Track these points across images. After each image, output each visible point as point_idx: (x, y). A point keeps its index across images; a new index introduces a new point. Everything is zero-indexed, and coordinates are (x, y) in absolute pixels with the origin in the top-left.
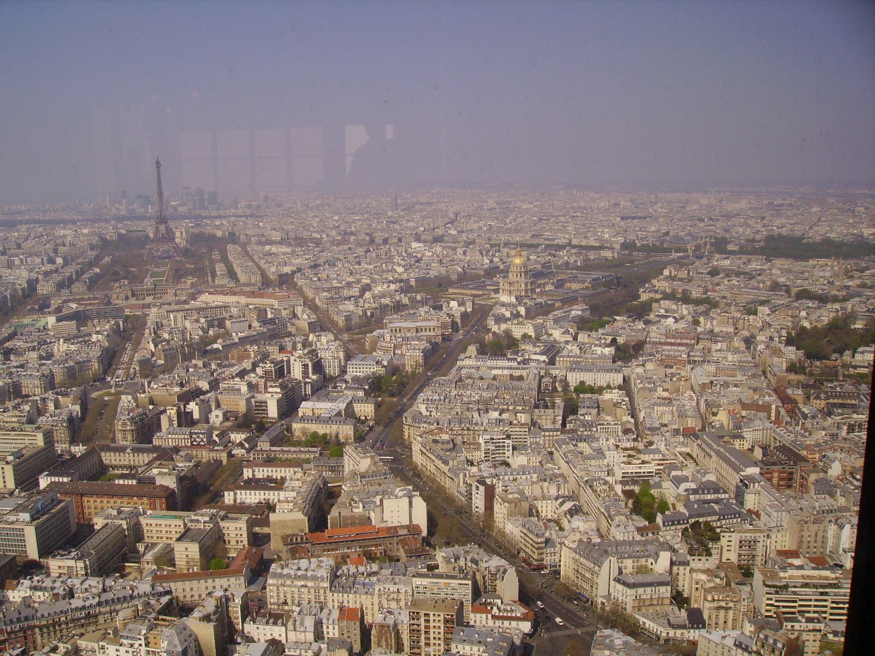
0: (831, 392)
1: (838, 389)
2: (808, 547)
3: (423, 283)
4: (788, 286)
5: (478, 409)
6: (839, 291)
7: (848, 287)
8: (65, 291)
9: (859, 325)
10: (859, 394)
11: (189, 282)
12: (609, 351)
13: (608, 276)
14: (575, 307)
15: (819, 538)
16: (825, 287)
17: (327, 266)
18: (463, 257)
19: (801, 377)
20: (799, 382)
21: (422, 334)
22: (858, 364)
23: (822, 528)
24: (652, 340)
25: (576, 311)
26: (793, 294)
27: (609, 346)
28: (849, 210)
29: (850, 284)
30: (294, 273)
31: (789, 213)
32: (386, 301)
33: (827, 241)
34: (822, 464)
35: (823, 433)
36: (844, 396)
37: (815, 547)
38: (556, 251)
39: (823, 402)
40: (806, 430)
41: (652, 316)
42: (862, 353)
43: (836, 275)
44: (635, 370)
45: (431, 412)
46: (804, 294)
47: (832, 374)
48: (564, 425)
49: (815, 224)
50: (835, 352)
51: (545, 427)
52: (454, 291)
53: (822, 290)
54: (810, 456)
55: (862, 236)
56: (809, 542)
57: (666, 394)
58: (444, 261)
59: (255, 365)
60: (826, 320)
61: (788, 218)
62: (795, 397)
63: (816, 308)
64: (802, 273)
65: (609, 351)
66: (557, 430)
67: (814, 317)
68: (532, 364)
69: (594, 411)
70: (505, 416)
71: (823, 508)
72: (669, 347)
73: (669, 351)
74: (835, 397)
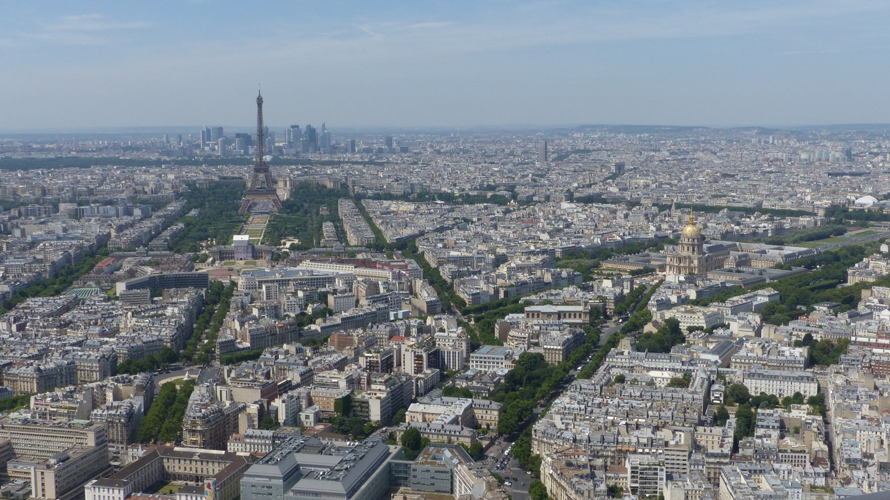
3: (571, 253)
5: (627, 424)
8: (141, 249)
11: (288, 245)
12: (800, 353)
13: (805, 252)
14: (760, 292)
17: (455, 230)
18: (622, 221)
21: (564, 321)
24: (859, 339)
25: (763, 297)
27: (798, 344)
32: (523, 277)
38: (742, 216)
41: (861, 308)
44: (833, 379)
45: (568, 424)
48: (735, 449)
51: (710, 451)
52: (610, 266)
57: (873, 414)
58: (600, 227)
59: (358, 354)
65: (800, 353)
66: (725, 456)
68: (701, 366)
69: (775, 434)
70: (660, 434)
72: (880, 351)
73: (880, 355)
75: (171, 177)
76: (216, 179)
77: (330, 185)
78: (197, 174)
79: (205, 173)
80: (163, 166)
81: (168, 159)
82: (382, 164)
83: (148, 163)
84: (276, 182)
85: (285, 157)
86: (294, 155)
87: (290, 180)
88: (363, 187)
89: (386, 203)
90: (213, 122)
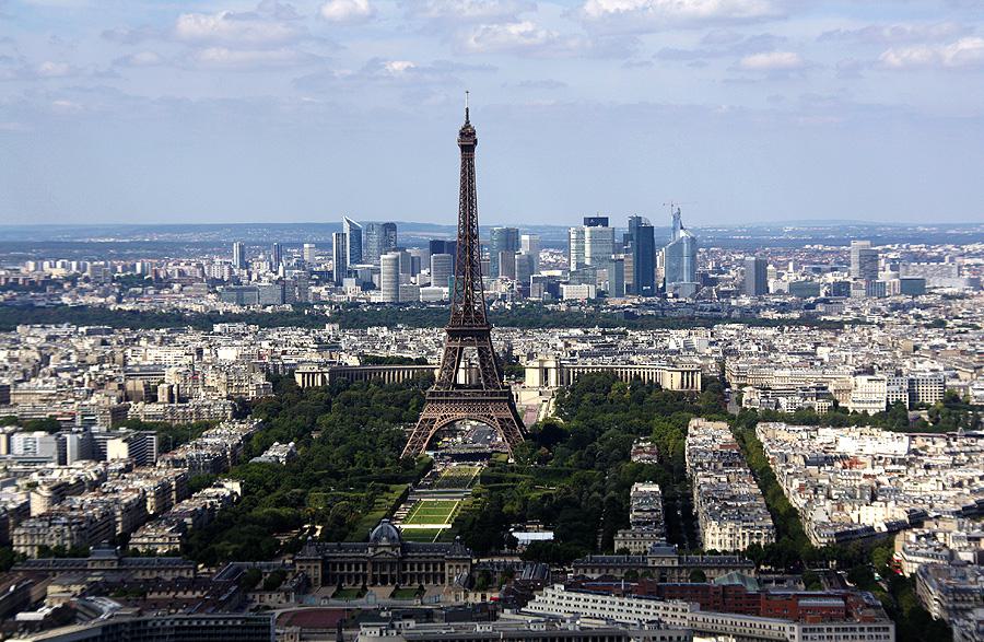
30: (895, 528)
75: (228, 354)
76: (353, 362)
77: (671, 381)
78: (303, 355)
79: (322, 346)
80: (217, 328)
81: (236, 310)
82: (837, 327)
83: (176, 321)
84: (521, 374)
85: (563, 307)
86: (590, 301)
87: (560, 367)
88: (765, 389)
89: (827, 434)
90: (372, 211)
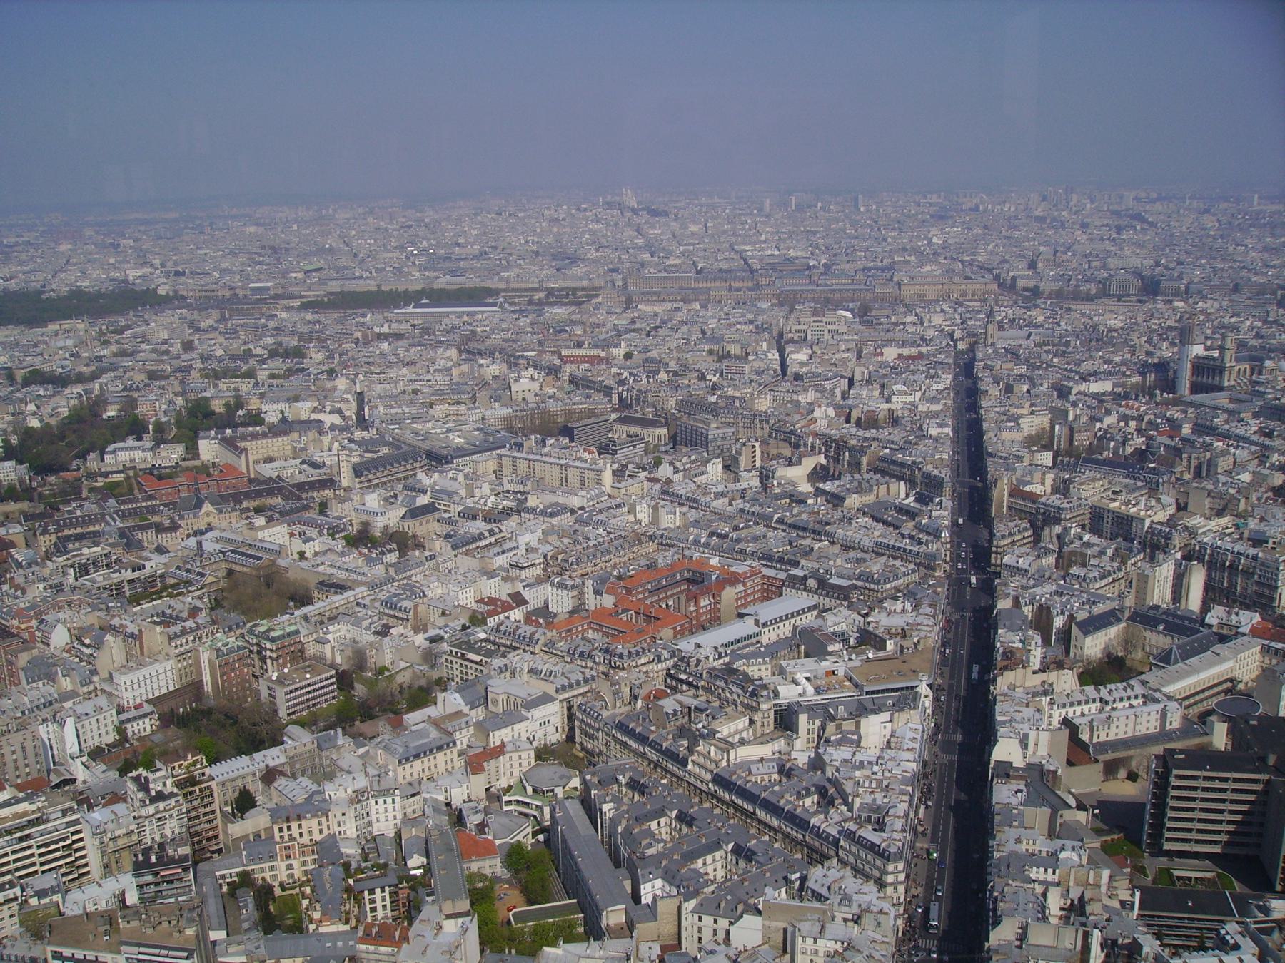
0: (70, 519)
1: (78, 513)
2: (17, 769)
4: (9, 368)
6: (87, 365)
7: (99, 359)
9: (111, 412)
10: (103, 515)
15: (30, 752)
16: (67, 363)
19: (24, 505)
20: (22, 512)
22: (109, 469)
23: (29, 736)
26: (19, 379)
28: (112, 244)
29: (104, 352)
31: (24, 256)
33: (78, 294)
34: (40, 635)
35: (41, 586)
36: (84, 521)
37: (27, 766)
39: (53, 537)
40: (17, 587)
42: (114, 452)
43: (82, 343)
46: (36, 377)
47: (72, 492)
49: (61, 270)
50: (77, 457)
53: (63, 367)
54: (23, 626)
55: (126, 281)
56: (15, 761)
60: (64, 412)
61: (21, 263)
62: (11, 538)
63: (50, 397)
64: (36, 345)
67: (47, 410)
71: (37, 703)
74: (71, 525)
